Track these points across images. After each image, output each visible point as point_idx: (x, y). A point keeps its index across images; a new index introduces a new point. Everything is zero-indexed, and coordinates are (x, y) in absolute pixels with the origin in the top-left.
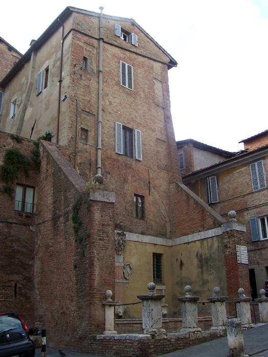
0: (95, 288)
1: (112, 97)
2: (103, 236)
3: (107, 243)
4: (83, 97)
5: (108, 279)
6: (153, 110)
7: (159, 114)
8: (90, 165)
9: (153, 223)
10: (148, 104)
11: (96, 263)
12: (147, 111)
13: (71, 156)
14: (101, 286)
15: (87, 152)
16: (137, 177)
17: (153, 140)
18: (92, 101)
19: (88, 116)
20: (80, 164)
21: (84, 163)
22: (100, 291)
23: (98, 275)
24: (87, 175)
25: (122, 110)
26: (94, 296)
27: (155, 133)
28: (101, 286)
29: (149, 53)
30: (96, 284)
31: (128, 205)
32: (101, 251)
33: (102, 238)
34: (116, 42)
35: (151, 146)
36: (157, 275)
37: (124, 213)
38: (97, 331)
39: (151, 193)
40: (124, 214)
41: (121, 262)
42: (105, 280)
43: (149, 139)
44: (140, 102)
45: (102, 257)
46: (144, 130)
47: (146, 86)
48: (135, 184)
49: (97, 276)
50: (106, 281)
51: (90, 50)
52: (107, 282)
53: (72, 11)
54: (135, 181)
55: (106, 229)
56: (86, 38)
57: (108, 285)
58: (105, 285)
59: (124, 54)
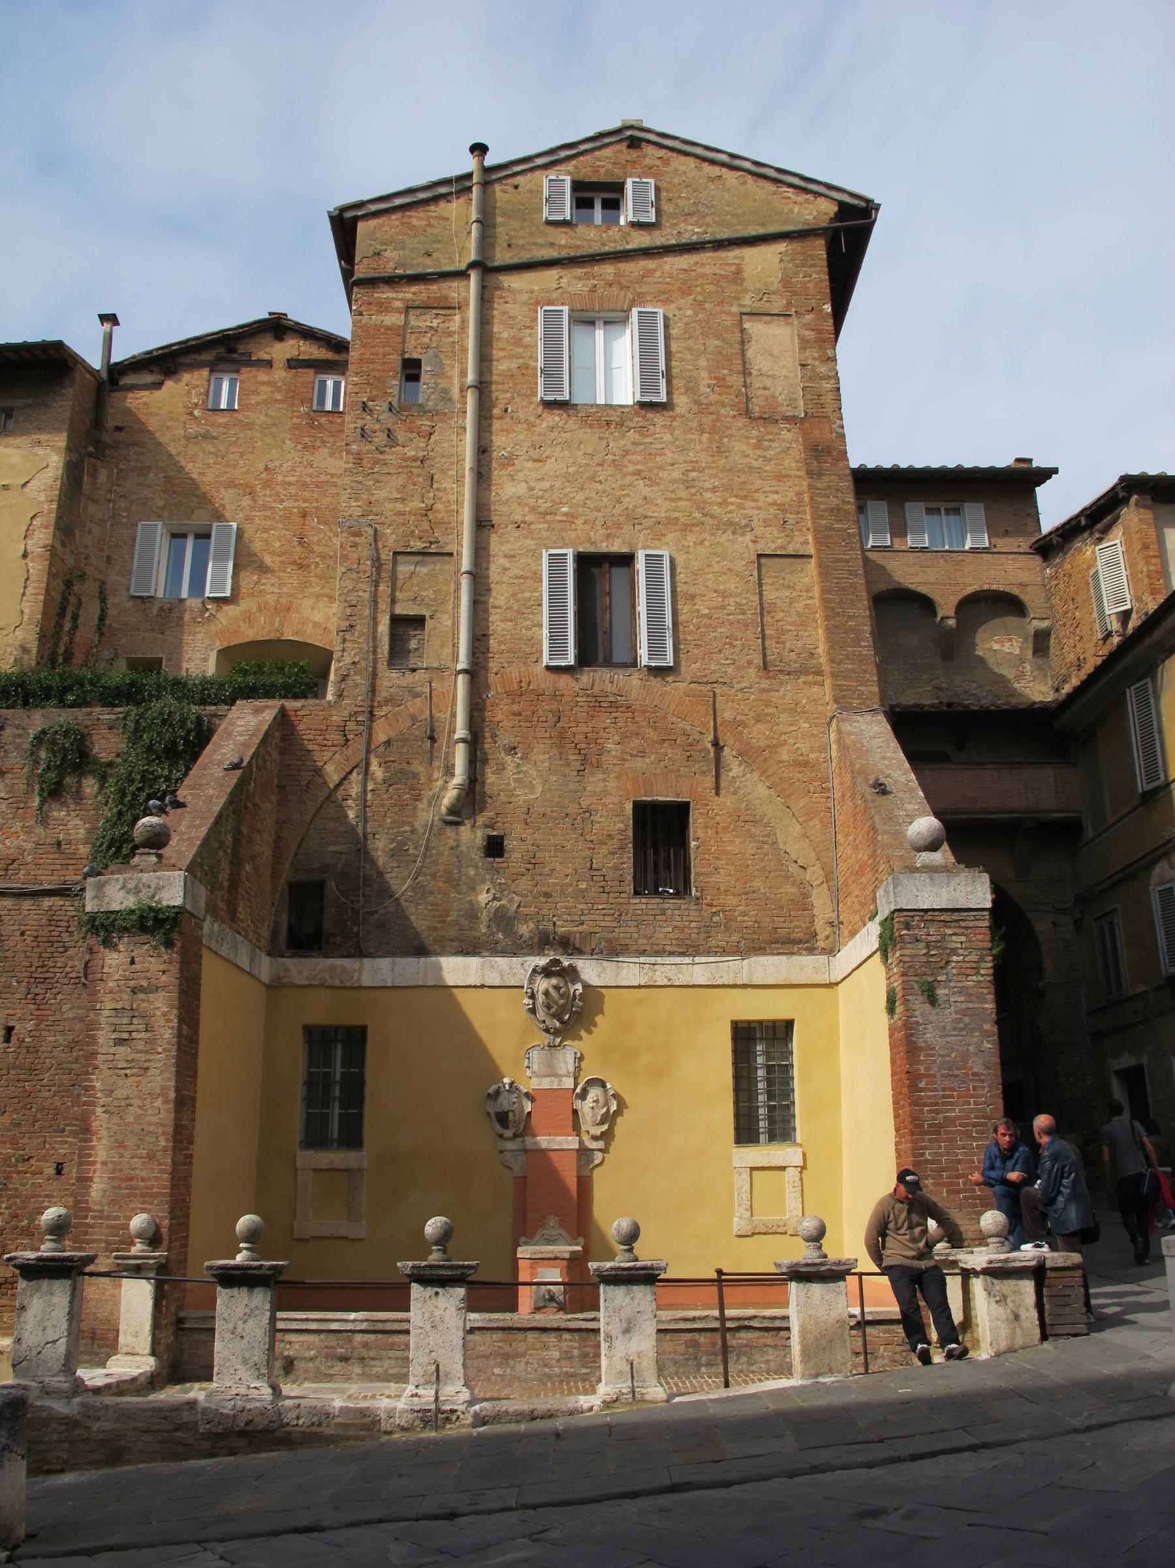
0: (89, 1210)
1: (530, 464)
2: (132, 1027)
3: (146, 1052)
4: (400, 507)
5: (144, 1174)
6: (739, 446)
7: (768, 454)
8: (432, 739)
9: (732, 901)
10: (714, 430)
11: (100, 1121)
12: (705, 459)
13: (351, 726)
14: (113, 1202)
15: (417, 695)
16: (651, 734)
17: (739, 566)
18: (439, 506)
19: (423, 564)
20: (388, 743)
21: (404, 740)
22: (108, 1218)
23: (104, 1163)
24: (415, 776)
25: (580, 497)
26: (86, 1233)
27: (748, 537)
28: (113, 1202)
29: (721, 224)
30: (93, 1194)
31: (604, 850)
32: (121, 1082)
33: (126, 1035)
34: (552, 245)
35: (724, 595)
36: (771, 1109)
37: (583, 885)
38: (90, 1354)
39: (723, 784)
40: (585, 890)
41: (563, 1071)
42: (132, 1179)
43: (716, 568)
44: (667, 437)
45: (123, 1103)
46: (691, 539)
47: (702, 363)
48: (639, 764)
49: (98, 1166)
50: (134, 1183)
51: (435, 323)
52: (137, 1188)
53: (355, 220)
54: (642, 753)
55: (145, 1005)
56: (410, 293)
57: (143, 1195)
58: (129, 1196)
59: (588, 277)
